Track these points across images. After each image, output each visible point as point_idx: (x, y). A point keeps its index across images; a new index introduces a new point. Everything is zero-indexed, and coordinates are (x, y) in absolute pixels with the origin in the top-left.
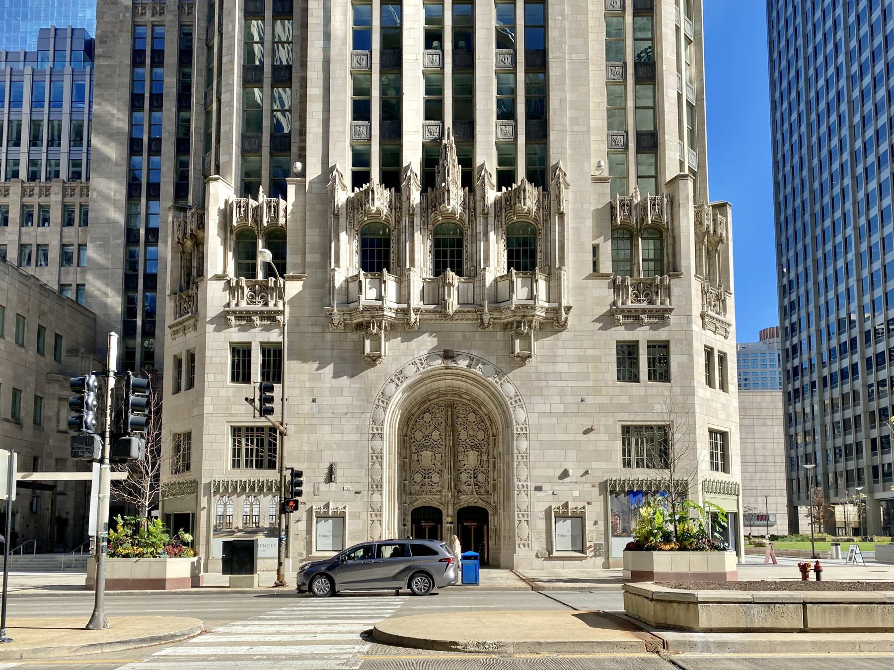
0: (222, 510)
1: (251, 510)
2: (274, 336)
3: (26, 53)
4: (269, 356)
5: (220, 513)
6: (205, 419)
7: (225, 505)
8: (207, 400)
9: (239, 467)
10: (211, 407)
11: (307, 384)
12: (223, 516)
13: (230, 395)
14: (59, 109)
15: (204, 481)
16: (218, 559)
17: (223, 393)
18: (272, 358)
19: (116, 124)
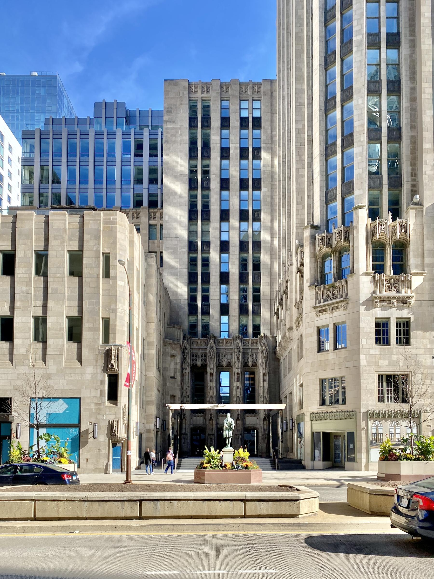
0: (375, 430)
1: (395, 430)
2: (405, 314)
3: (53, 119)
4: (400, 327)
5: (374, 432)
6: (361, 370)
7: (377, 427)
8: (362, 357)
9: (383, 401)
10: (365, 361)
11: (429, 346)
12: (376, 434)
13: (377, 353)
14: (114, 158)
15: (363, 410)
16: (375, 462)
17: (372, 352)
18: (382, 329)
19: (179, 169)
